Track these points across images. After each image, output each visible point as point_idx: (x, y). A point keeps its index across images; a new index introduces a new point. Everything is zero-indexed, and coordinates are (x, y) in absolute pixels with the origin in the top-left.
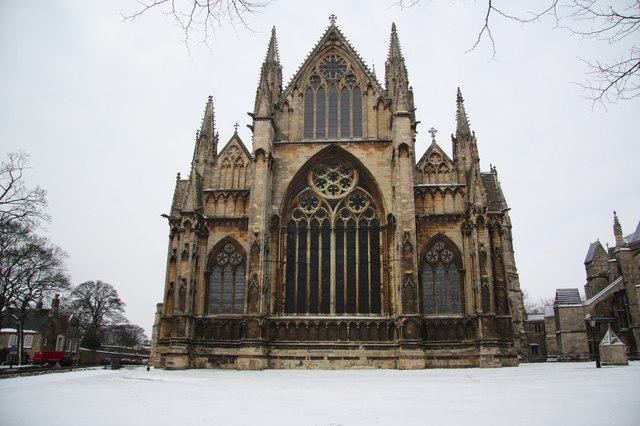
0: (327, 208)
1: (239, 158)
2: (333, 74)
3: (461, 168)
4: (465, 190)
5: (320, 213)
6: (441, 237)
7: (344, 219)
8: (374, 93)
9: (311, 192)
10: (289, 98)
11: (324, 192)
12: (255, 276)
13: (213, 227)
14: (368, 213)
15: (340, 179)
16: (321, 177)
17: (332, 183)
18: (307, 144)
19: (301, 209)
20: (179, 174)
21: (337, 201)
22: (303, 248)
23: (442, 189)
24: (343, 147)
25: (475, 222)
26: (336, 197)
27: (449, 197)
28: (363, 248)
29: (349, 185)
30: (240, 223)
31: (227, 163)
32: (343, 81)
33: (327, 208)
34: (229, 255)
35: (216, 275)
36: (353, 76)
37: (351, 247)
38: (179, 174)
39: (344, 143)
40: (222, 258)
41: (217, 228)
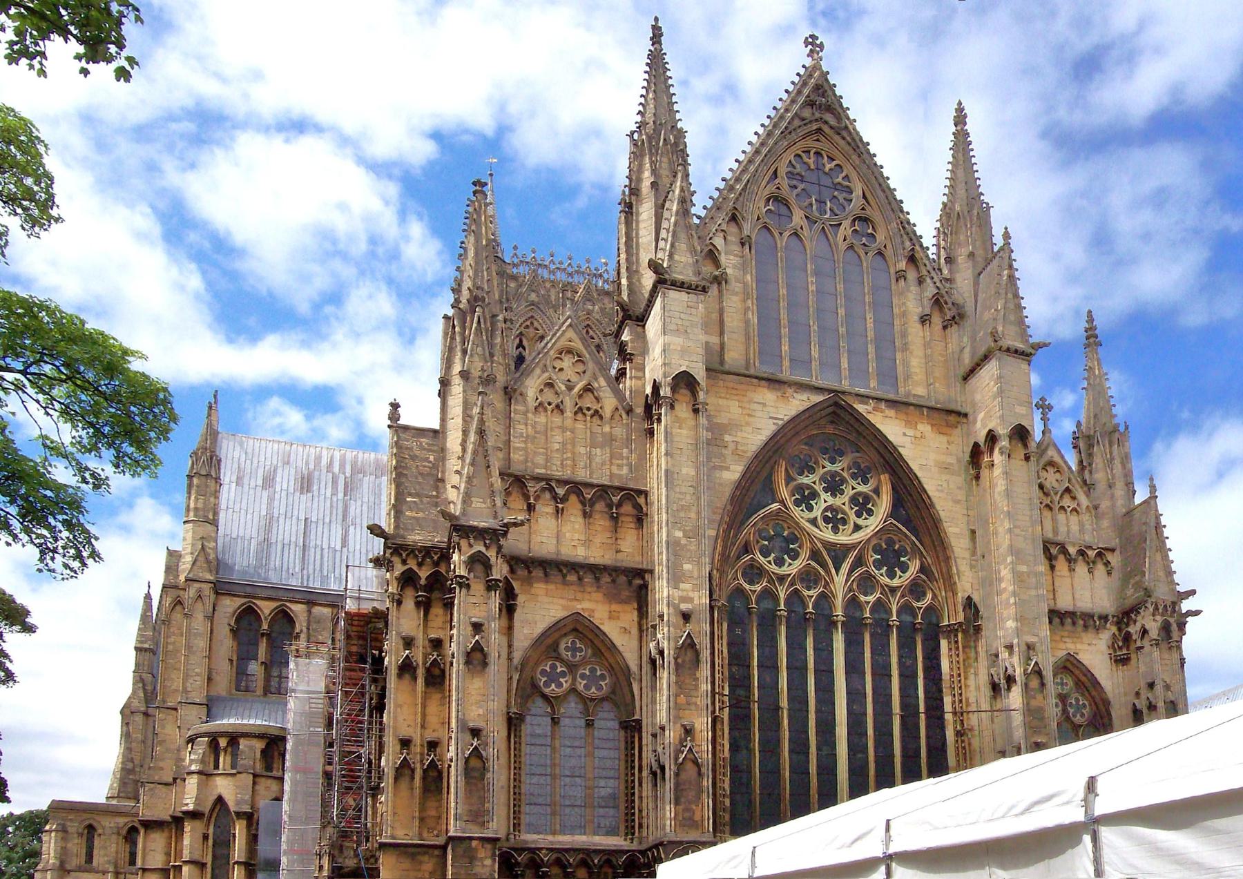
0: (823, 565)
1: (588, 389)
2: (821, 202)
3: (1105, 504)
4: (1113, 559)
5: (809, 577)
6: (1070, 666)
7: (863, 598)
8: (920, 281)
9: (781, 517)
10: (718, 241)
11: (813, 522)
12: (688, 731)
13: (528, 581)
14: (916, 589)
15: (849, 492)
16: (805, 480)
17: (831, 501)
18: (774, 382)
19: (761, 559)
20: (395, 406)
21: (847, 549)
22: (770, 665)
23: (1072, 550)
24: (861, 408)
25: (1154, 633)
26: (843, 538)
27: (1081, 568)
28: (908, 677)
29: (870, 513)
30: (606, 579)
31: (549, 396)
32: (846, 228)
33: (823, 565)
34: (572, 668)
35: (537, 723)
36: (865, 220)
37: (882, 673)
38: (395, 406)
39: (864, 398)
40: (553, 678)
41: (540, 588)
